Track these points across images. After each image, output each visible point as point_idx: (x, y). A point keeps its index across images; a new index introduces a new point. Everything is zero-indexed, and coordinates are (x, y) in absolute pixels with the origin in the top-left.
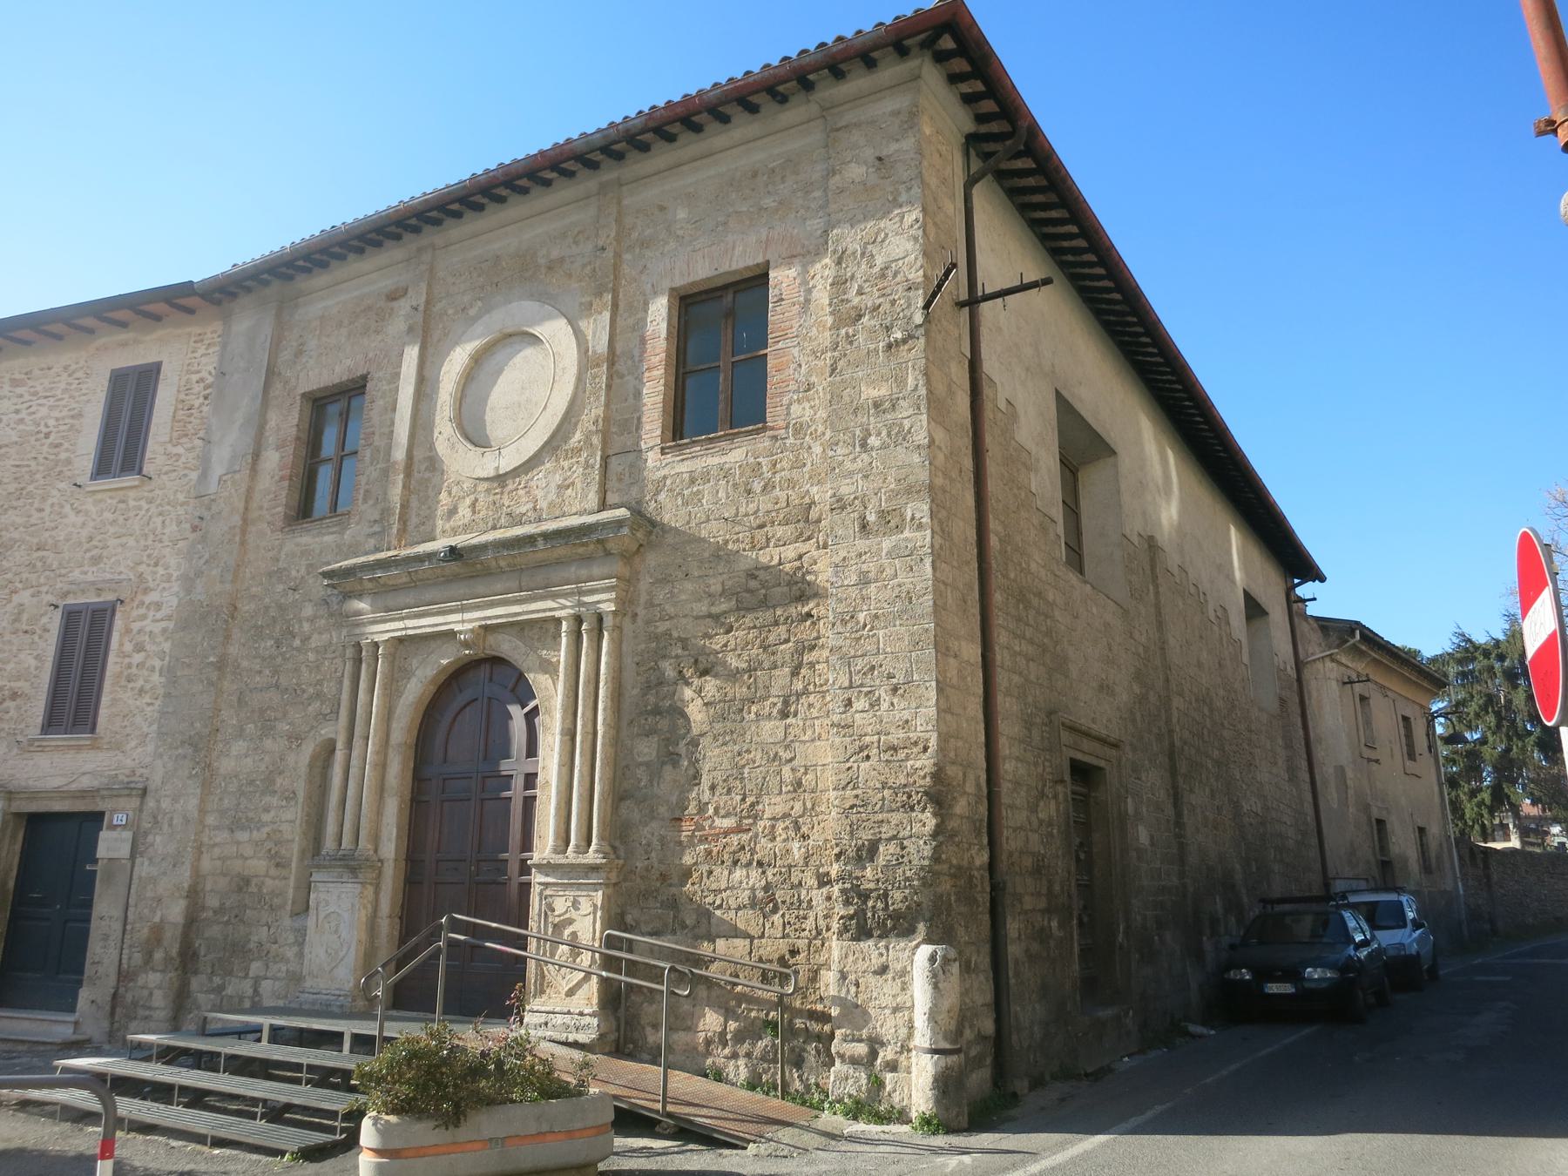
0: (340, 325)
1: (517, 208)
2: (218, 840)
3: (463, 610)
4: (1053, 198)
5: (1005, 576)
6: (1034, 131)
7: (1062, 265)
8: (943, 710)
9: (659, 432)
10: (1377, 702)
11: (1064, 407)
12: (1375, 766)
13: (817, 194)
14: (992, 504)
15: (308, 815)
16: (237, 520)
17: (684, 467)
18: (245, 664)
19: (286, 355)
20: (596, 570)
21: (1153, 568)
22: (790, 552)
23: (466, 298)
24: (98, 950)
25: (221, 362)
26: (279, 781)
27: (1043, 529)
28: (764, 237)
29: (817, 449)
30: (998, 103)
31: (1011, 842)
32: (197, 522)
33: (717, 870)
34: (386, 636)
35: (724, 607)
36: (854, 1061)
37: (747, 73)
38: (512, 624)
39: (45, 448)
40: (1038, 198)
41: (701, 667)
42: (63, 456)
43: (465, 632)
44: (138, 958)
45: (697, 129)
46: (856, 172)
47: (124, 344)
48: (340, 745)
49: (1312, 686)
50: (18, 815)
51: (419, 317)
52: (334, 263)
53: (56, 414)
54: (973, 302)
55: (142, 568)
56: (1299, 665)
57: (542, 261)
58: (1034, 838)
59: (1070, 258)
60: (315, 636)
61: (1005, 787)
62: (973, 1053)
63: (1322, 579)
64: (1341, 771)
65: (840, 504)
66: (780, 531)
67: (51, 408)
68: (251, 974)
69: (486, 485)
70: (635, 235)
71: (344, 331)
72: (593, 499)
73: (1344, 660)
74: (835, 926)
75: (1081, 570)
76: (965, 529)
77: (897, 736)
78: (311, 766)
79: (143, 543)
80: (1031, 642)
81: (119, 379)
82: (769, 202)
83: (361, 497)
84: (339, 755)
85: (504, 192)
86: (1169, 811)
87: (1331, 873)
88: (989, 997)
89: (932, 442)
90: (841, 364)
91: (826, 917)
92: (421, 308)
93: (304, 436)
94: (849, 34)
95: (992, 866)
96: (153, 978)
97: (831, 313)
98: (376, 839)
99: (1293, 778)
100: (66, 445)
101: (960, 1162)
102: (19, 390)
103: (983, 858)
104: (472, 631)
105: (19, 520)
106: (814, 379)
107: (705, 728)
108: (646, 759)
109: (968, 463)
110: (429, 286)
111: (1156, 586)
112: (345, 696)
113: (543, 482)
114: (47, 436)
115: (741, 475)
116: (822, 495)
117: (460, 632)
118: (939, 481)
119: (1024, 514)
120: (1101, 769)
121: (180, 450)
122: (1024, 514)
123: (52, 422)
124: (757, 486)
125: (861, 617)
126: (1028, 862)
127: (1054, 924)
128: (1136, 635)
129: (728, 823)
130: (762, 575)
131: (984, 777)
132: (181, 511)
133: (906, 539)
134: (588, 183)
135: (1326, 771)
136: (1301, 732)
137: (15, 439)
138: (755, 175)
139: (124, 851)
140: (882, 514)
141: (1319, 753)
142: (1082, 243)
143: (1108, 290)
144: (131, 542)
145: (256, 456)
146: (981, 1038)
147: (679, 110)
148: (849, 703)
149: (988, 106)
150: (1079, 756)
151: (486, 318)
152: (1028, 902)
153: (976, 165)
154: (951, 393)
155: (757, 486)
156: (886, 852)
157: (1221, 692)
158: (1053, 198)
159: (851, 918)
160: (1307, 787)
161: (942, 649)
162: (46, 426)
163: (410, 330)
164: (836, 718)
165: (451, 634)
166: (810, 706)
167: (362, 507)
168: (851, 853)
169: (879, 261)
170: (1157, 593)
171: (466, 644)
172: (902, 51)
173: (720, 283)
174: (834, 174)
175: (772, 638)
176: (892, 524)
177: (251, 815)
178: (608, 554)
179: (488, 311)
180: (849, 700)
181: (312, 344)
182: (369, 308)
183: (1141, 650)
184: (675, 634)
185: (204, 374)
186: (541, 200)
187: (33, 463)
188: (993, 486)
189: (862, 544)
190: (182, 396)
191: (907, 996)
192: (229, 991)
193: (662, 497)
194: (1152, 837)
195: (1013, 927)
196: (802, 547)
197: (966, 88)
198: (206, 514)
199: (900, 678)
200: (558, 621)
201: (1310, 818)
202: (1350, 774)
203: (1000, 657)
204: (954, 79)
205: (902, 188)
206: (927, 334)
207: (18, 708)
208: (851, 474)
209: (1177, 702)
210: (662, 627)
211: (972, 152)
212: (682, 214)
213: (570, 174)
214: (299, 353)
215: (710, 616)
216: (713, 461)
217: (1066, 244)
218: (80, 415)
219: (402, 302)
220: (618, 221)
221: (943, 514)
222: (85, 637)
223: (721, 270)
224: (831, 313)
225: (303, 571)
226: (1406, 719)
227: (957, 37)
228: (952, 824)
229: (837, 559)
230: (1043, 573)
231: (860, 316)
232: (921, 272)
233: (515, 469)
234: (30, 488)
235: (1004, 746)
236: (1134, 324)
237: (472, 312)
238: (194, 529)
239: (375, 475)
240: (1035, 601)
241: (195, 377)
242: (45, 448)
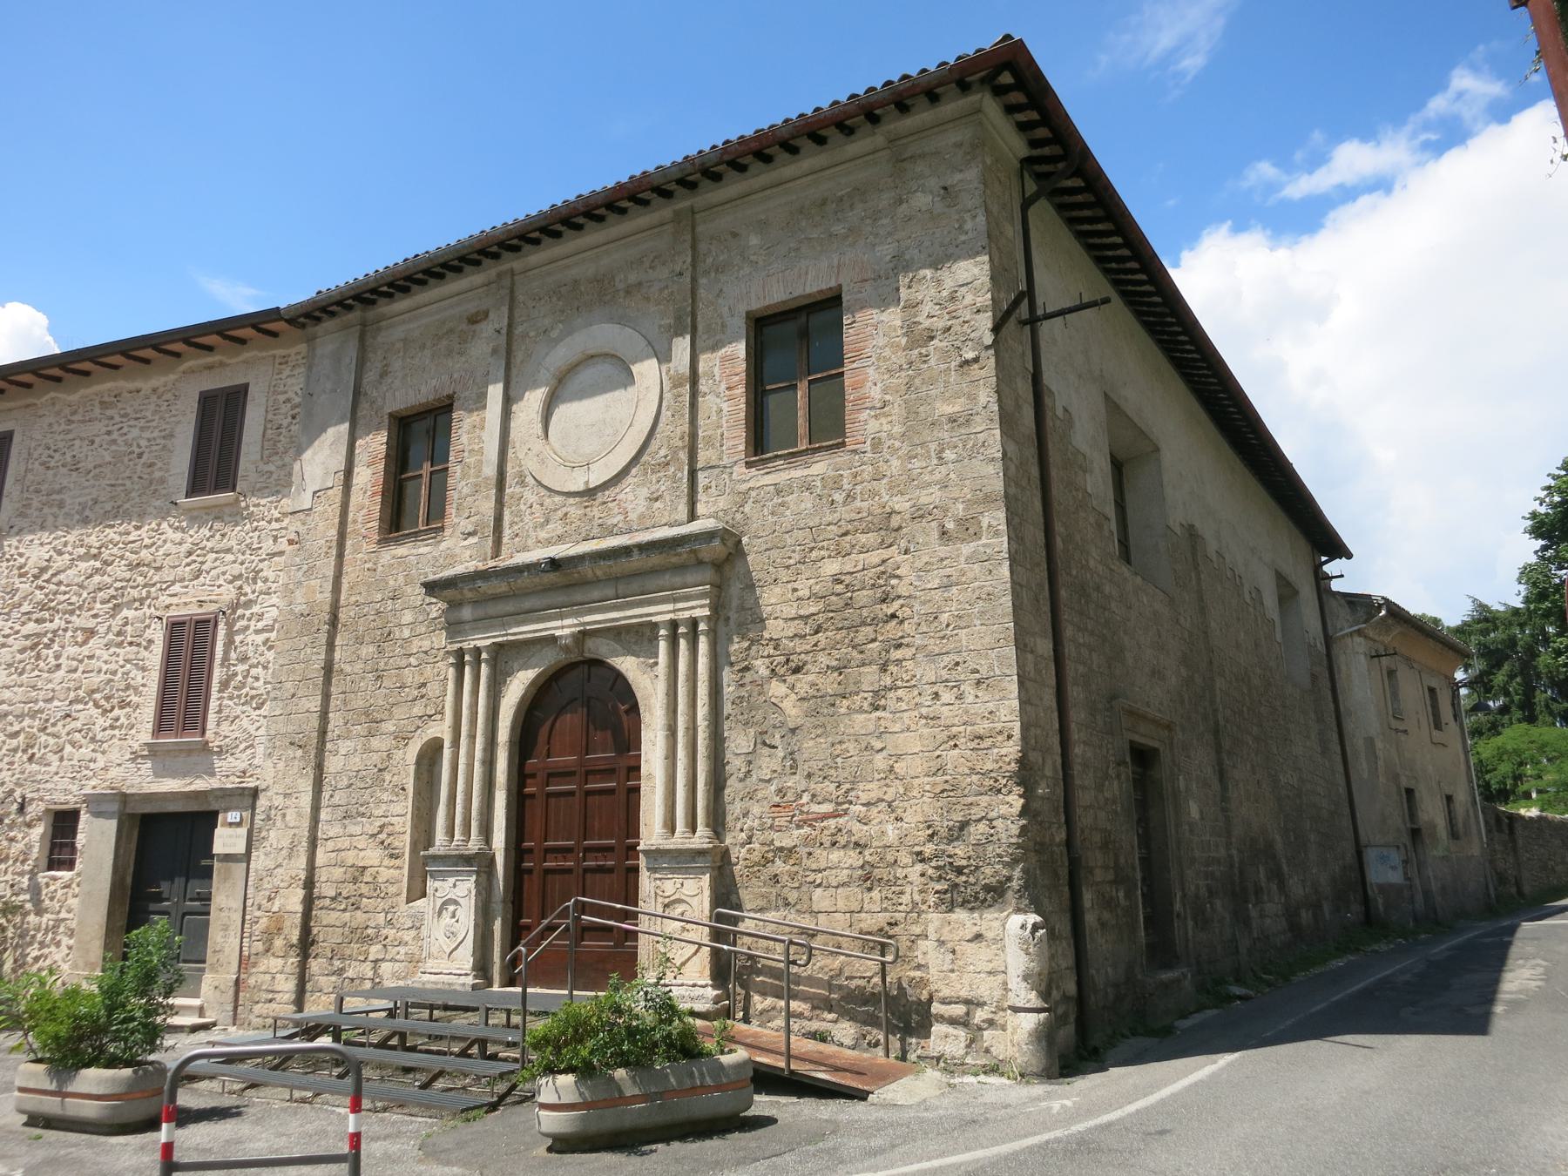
0: (423, 347)
1: (593, 236)
2: (331, 834)
3: (561, 617)
4: (1100, 212)
5: (1069, 574)
6: (1086, 153)
7: (1116, 283)
8: (1024, 702)
9: (742, 447)
10: (1403, 674)
11: (1113, 406)
12: (1403, 737)
13: (885, 221)
14: (1056, 507)
16: (333, 532)
18: (347, 668)
19: (370, 376)
20: (690, 578)
21: (1194, 554)
22: (874, 557)
23: (547, 321)
24: (219, 939)
25: (307, 383)
26: (388, 777)
27: (1099, 526)
28: (836, 262)
29: (895, 463)
30: (1052, 130)
31: (1084, 820)
32: (293, 536)
33: (818, 852)
34: (488, 642)
35: (813, 610)
36: (953, 1021)
37: (817, 109)
38: (609, 629)
39: (139, 468)
40: (1087, 213)
41: (793, 665)
42: (157, 475)
43: (566, 637)
44: (259, 946)
45: (768, 159)
46: (922, 200)
47: (210, 367)
48: (447, 744)
49: (1341, 660)
50: (132, 816)
51: (503, 339)
52: (415, 288)
53: (147, 435)
54: (1033, 321)
55: (238, 583)
56: (1328, 640)
57: (621, 286)
58: (1102, 815)
59: (1114, 265)
60: (416, 643)
61: (1077, 769)
62: (1060, 1011)
63: (1349, 556)
64: (1370, 742)
65: (919, 514)
66: (863, 538)
67: (142, 429)
68: (371, 958)
70: (709, 260)
71: (427, 352)
72: (682, 511)
73: (1371, 634)
74: (932, 899)
75: (1129, 562)
76: (1035, 534)
77: (983, 727)
78: (418, 763)
79: (241, 558)
80: (1092, 633)
81: (207, 401)
82: (839, 229)
84: (447, 753)
85: (581, 220)
86: (1216, 786)
87: (1363, 839)
88: (1071, 961)
89: (1005, 454)
90: (917, 381)
91: (921, 892)
92: (504, 331)
93: (393, 453)
94: (914, 73)
95: (1069, 843)
96: (275, 964)
97: (906, 334)
99: (1325, 751)
100: (160, 464)
101: (1063, 1106)
102: (109, 412)
103: (1061, 836)
104: (573, 635)
105: (117, 538)
106: (887, 397)
107: (800, 721)
109: (1035, 471)
110: (511, 310)
111: (1198, 574)
112: (449, 698)
113: (633, 496)
114: (140, 456)
115: (824, 487)
116: (901, 504)
118: (1012, 491)
119: (1082, 514)
120: (1156, 750)
121: (271, 467)
122: (1082, 514)
123: (143, 443)
124: (839, 497)
125: (944, 617)
126: (1097, 838)
127: (1121, 894)
128: (1182, 621)
129: (827, 808)
130: (848, 579)
131: (1059, 760)
132: (275, 525)
133: (984, 546)
134: (663, 212)
135: (1357, 743)
136: (1332, 706)
137: (108, 459)
138: (824, 202)
139: (240, 848)
140: (959, 522)
141: (1349, 726)
142: (1126, 252)
143: (1149, 294)
144: (230, 557)
145: (349, 473)
146: (1065, 998)
147: (753, 145)
148: (936, 695)
149: (1042, 133)
150: (1137, 738)
151: (568, 340)
152: (1099, 875)
153: (1031, 187)
154: (1018, 407)
155: (839, 497)
156: (978, 831)
157: (1258, 671)
158: (1100, 212)
159: (946, 892)
160: (1338, 759)
161: (1021, 646)
162: (139, 446)
163: (495, 352)
164: (924, 711)
165: (553, 640)
166: (899, 699)
167: (456, 520)
168: (943, 832)
169: (949, 284)
170: (1199, 579)
171: (566, 649)
172: (964, 87)
173: (794, 305)
174: (900, 201)
175: (860, 638)
176: (971, 531)
177: (362, 809)
178: (700, 563)
179: (570, 333)
180: (936, 694)
181: (397, 365)
182: (451, 331)
183: (1186, 635)
185: (291, 395)
186: (617, 228)
187: (128, 482)
188: (1056, 490)
189: (943, 551)
190: (270, 416)
191: (994, 961)
192: (350, 973)
193: (747, 509)
194: (1201, 812)
195: (1088, 898)
196: (885, 554)
197: (1021, 117)
198: (302, 529)
199: (984, 673)
200: (655, 626)
201: (1342, 790)
202: (1379, 745)
203: (1069, 649)
204: (1010, 109)
205: (967, 216)
206: (997, 355)
207: (128, 717)
208: (929, 484)
209: (1220, 683)
211: (1026, 175)
212: (754, 240)
213: (645, 203)
214: (384, 374)
215: (801, 617)
216: (797, 473)
217: (1110, 253)
218: (172, 436)
219: (483, 325)
220: (694, 247)
221: (1017, 520)
222: (190, 651)
223: (796, 294)
224: (906, 334)
225: (401, 579)
226: (1432, 691)
227: (1015, 74)
228: (1035, 805)
229: (919, 564)
230: (1100, 568)
231: (932, 338)
232: (989, 295)
233: (605, 483)
234: (127, 506)
235: (1076, 734)
236: (1172, 324)
237: (554, 334)
238: (291, 542)
239: (466, 491)
240: (1094, 595)
241: (282, 398)
242: (139, 468)
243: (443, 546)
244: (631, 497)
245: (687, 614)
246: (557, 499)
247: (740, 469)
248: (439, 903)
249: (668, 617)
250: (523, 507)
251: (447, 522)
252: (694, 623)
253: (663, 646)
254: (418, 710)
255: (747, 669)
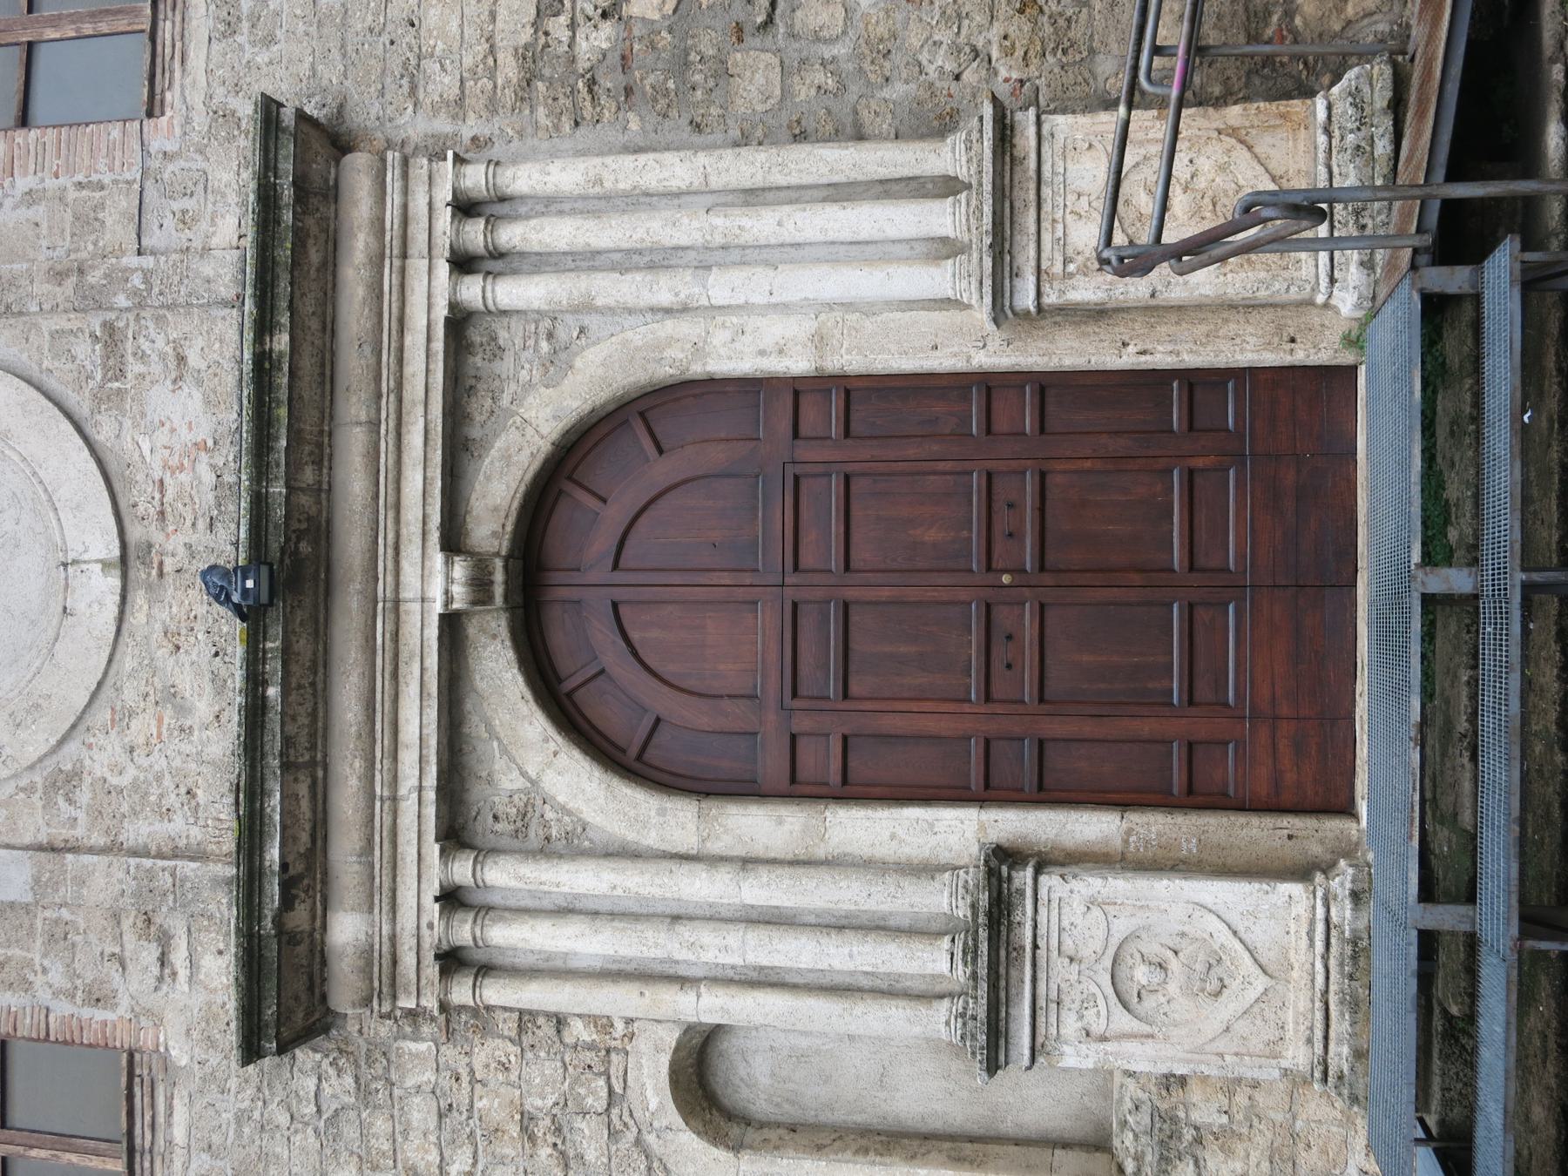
15: (866, 1151)
17: (197, 59)
43: (449, 580)
69: (139, 599)
78: (737, 1147)
83: (100, 1015)
98: (925, 870)
104: (448, 563)
108: (776, 76)
117: (449, 598)
165: (452, 625)
167: (123, 1010)
171: (480, 586)
184: (526, 35)
200: (459, 322)
210: (509, 69)
243: (180, 1055)
244: (162, 437)
245: (445, 217)
246: (127, 662)
247: (163, 134)
248: (1123, 1021)
249: (443, 269)
250: (131, 772)
251: (123, 1039)
252: (465, 208)
253: (510, 292)
254: (589, 1139)
255: (592, 84)
